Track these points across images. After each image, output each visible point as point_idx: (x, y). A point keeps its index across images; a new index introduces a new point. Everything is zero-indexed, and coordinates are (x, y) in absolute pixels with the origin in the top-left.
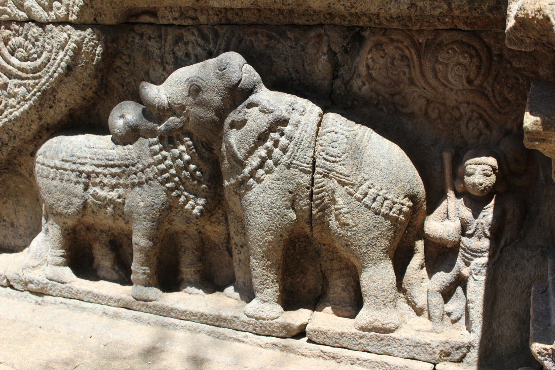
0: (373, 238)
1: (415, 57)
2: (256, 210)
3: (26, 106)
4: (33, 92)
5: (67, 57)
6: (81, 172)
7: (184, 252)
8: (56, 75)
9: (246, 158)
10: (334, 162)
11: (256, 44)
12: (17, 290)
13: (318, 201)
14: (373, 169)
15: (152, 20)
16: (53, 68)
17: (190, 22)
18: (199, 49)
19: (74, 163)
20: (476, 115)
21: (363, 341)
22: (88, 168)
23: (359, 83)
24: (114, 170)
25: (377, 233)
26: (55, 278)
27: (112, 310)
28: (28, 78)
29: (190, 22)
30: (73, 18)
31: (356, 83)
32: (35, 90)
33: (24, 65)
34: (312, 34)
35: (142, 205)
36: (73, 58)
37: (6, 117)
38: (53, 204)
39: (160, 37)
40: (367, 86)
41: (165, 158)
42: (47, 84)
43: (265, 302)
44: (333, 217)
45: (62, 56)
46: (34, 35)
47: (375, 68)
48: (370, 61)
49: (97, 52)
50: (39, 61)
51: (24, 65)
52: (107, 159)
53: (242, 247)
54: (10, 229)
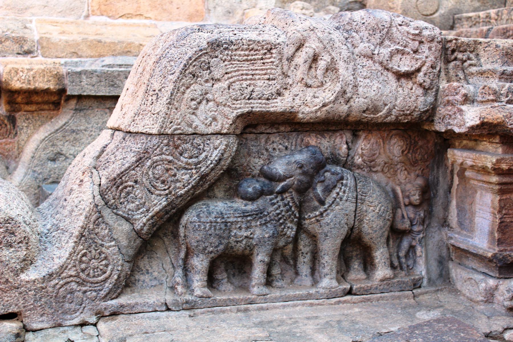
1: (382, 143)
3: (190, 186)
4: (195, 177)
6: (227, 223)
7: (275, 264)
8: (212, 165)
10: (365, 196)
11: (310, 142)
12: (174, 311)
15: (254, 131)
16: (210, 162)
17: (275, 131)
18: (280, 146)
19: (223, 218)
20: (404, 168)
21: (382, 287)
22: (231, 220)
23: (358, 157)
24: (249, 218)
25: (384, 230)
26: (204, 295)
27: (243, 307)
28: (192, 169)
29: (275, 131)
30: (225, 131)
31: (356, 157)
32: (196, 176)
33: (190, 161)
34: (338, 134)
36: (222, 154)
37: (174, 195)
39: (256, 139)
41: (279, 206)
43: (332, 279)
44: (365, 225)
46: (198, 142)
48: (363, 146)
51: (190, 161)
52: (244, 213)
53: (307, 254)
54: (147, 276)
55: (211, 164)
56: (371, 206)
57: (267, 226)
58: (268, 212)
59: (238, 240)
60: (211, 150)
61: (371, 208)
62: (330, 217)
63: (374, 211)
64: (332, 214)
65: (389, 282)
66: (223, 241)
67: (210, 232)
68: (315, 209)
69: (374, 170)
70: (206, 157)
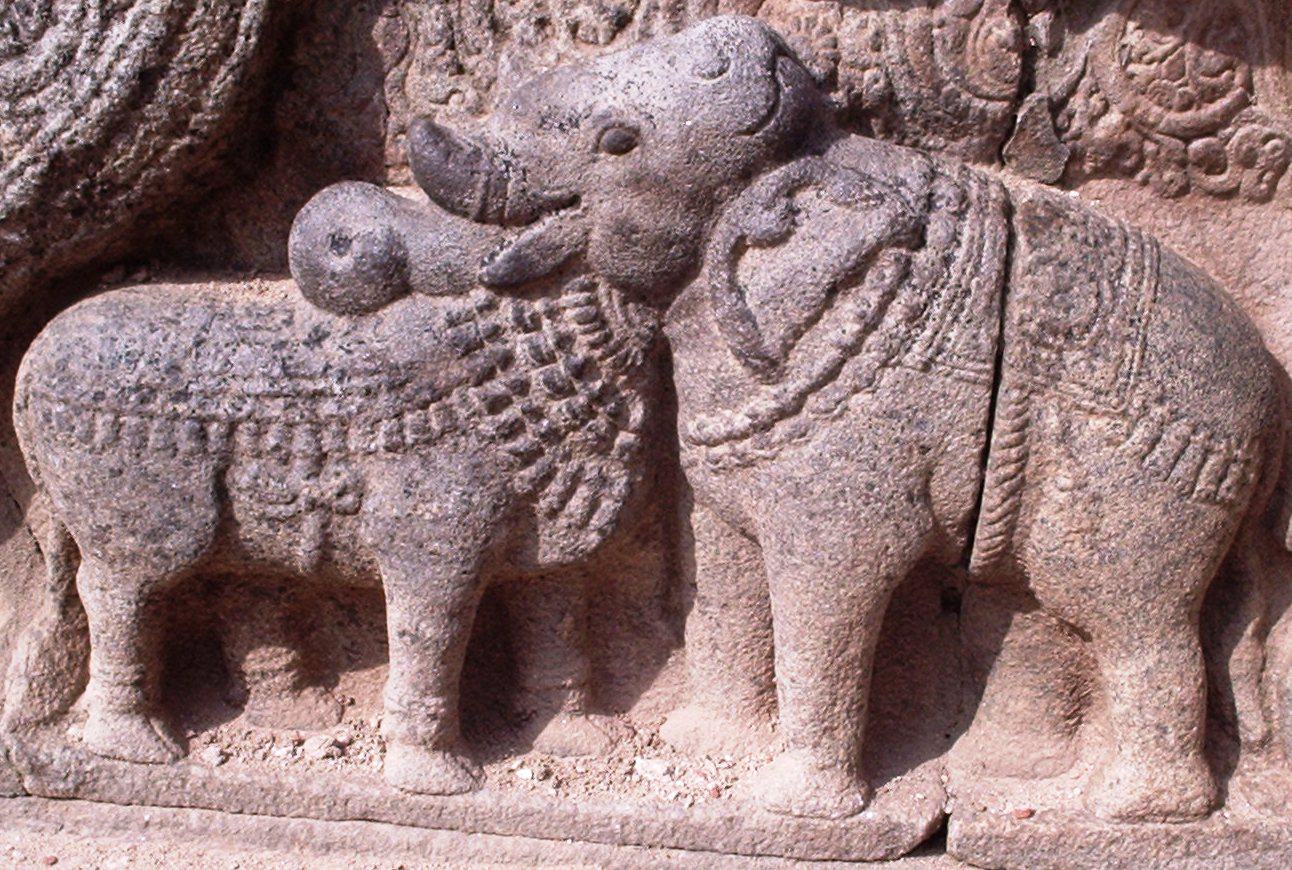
0: (1164, 569)
2: (815, 508)
4: (14, 164)
5: (135, 46)
8: (97, 106)
9: (787, 348)
13: (1011, 469)
14: (1175, 367)
19: (183, 396)
32: (23, 156)
35: (428, 516)
36: (166, 46)
38: (109, 527)
40: (1114, 118)
42: (66, 135)
45: (119, 41)
47: (1147, 58)
49: (244, 23)
50: (34, 63)
55: (97, 92)
56: (1092, 412)
57: (425, 461)
58: (431, 387)
59: (272, 511)
60: (93, 17)
61: (1095, 423)
62: (809, 450)
63: (1110, 442)
64: (822, 435)
65: (1175, 830)
66: (184, 515)
67: (109, 460)
68: (723, 394)
69: (1216, 180)
70: (67, 56)
